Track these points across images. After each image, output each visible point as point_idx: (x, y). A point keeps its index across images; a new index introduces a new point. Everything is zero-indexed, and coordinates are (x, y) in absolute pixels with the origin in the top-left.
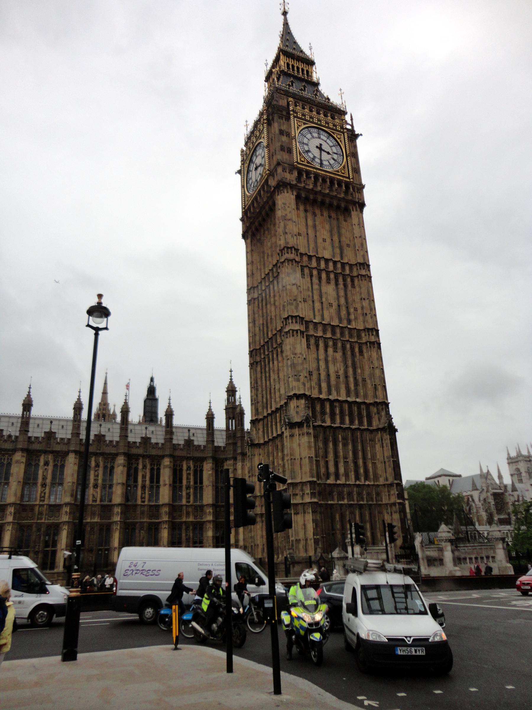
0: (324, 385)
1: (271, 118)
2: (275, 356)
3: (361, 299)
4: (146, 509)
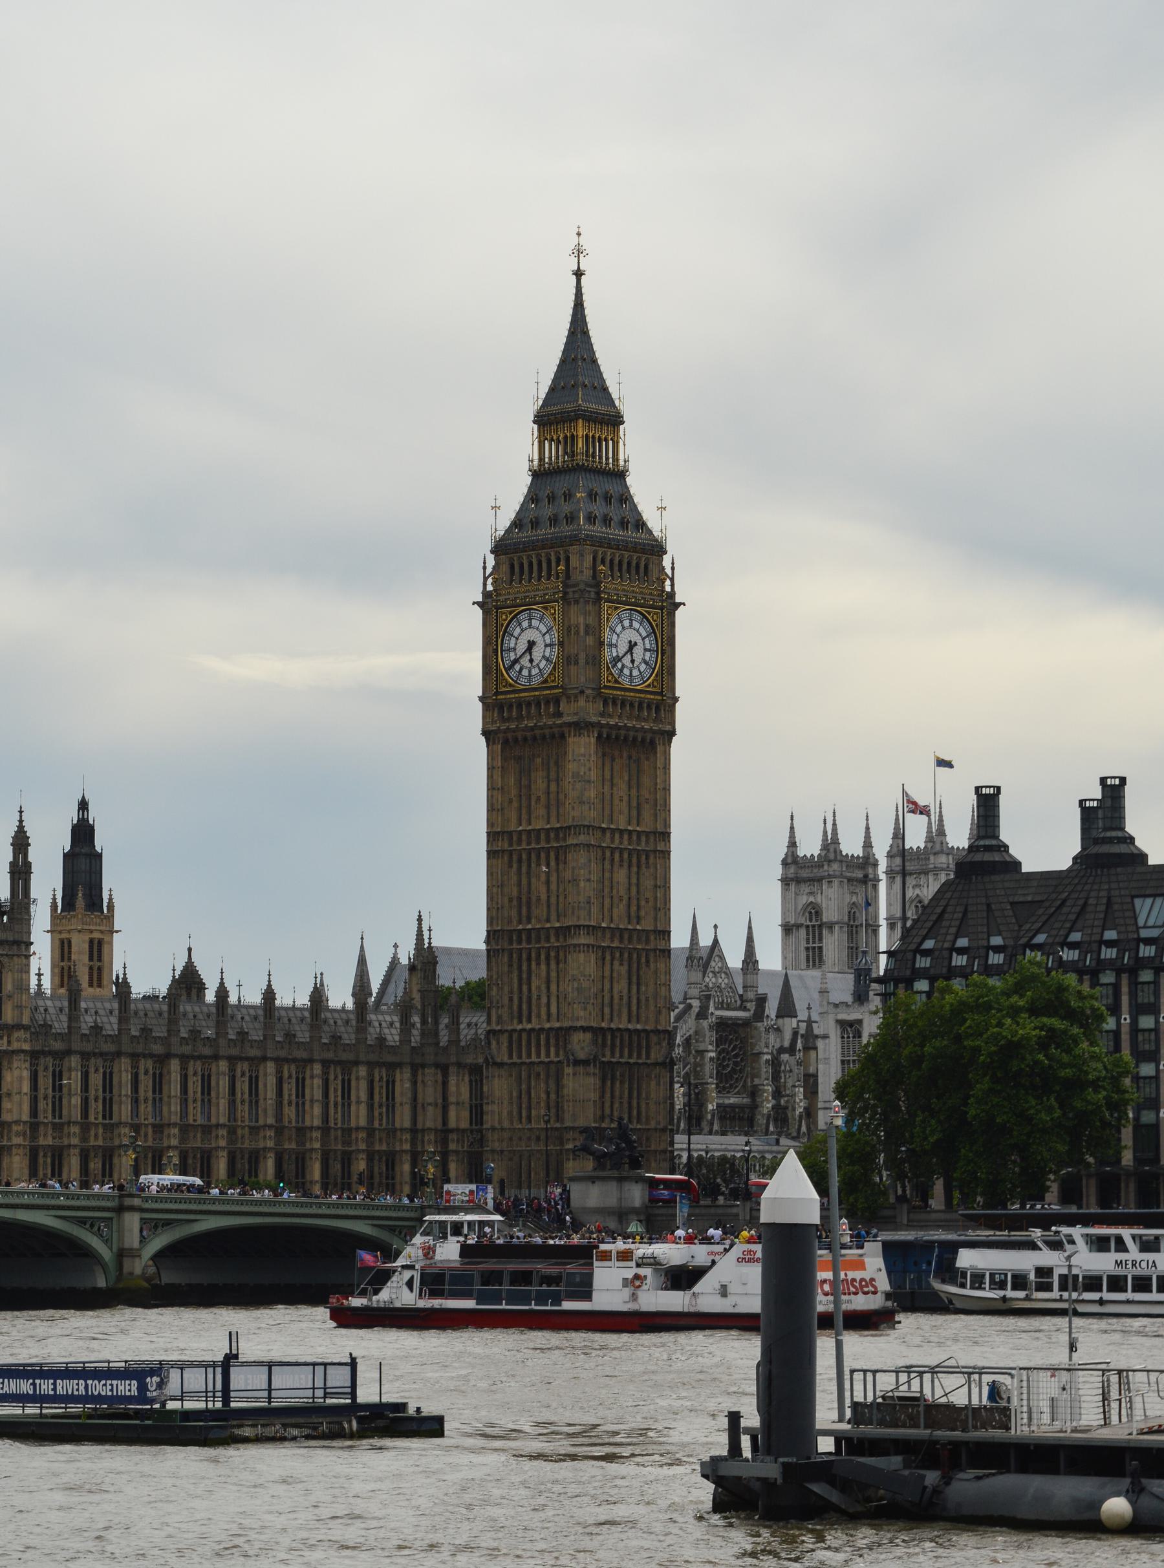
0: (607, 1010)
1: (571, 595)
2: (543, 957)
3: (656, 886)
4: (339, 1133)
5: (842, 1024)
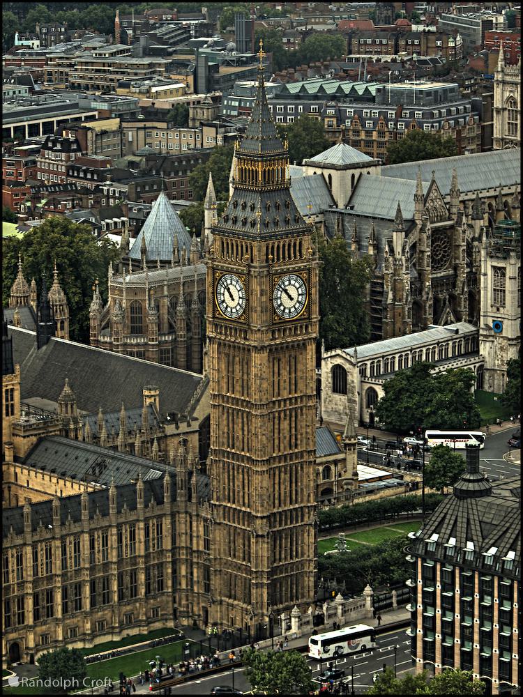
0: (277, 502)
1: (252, 273)
4: (129, 560)
5: (494, 267)
